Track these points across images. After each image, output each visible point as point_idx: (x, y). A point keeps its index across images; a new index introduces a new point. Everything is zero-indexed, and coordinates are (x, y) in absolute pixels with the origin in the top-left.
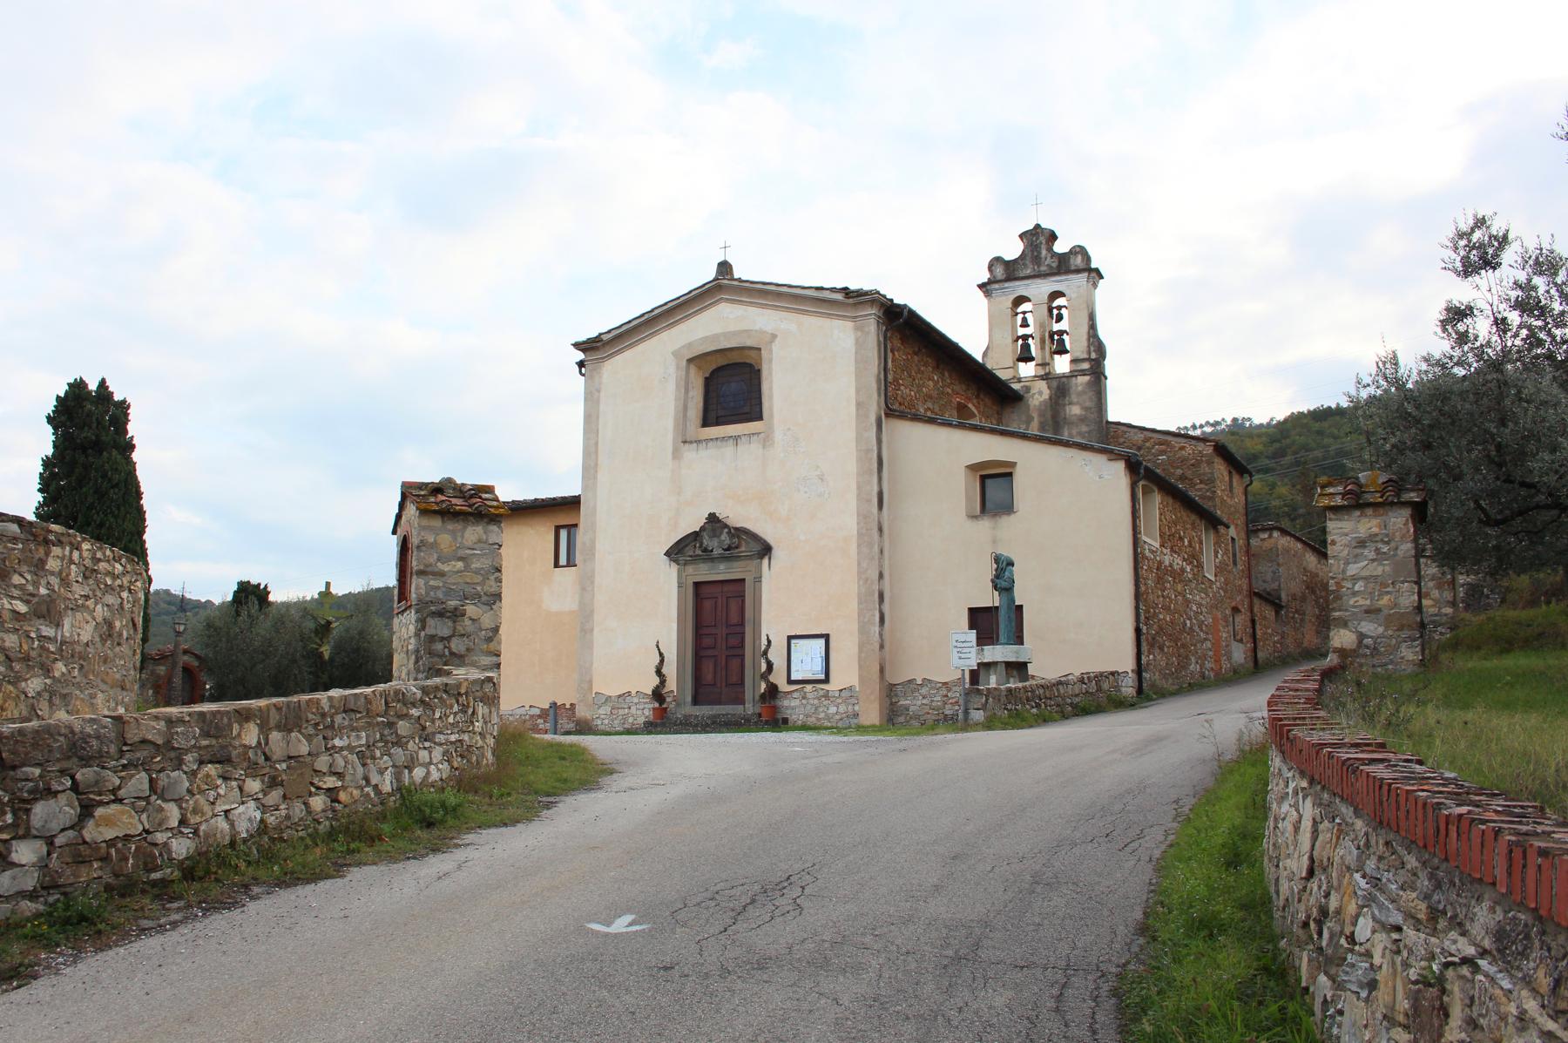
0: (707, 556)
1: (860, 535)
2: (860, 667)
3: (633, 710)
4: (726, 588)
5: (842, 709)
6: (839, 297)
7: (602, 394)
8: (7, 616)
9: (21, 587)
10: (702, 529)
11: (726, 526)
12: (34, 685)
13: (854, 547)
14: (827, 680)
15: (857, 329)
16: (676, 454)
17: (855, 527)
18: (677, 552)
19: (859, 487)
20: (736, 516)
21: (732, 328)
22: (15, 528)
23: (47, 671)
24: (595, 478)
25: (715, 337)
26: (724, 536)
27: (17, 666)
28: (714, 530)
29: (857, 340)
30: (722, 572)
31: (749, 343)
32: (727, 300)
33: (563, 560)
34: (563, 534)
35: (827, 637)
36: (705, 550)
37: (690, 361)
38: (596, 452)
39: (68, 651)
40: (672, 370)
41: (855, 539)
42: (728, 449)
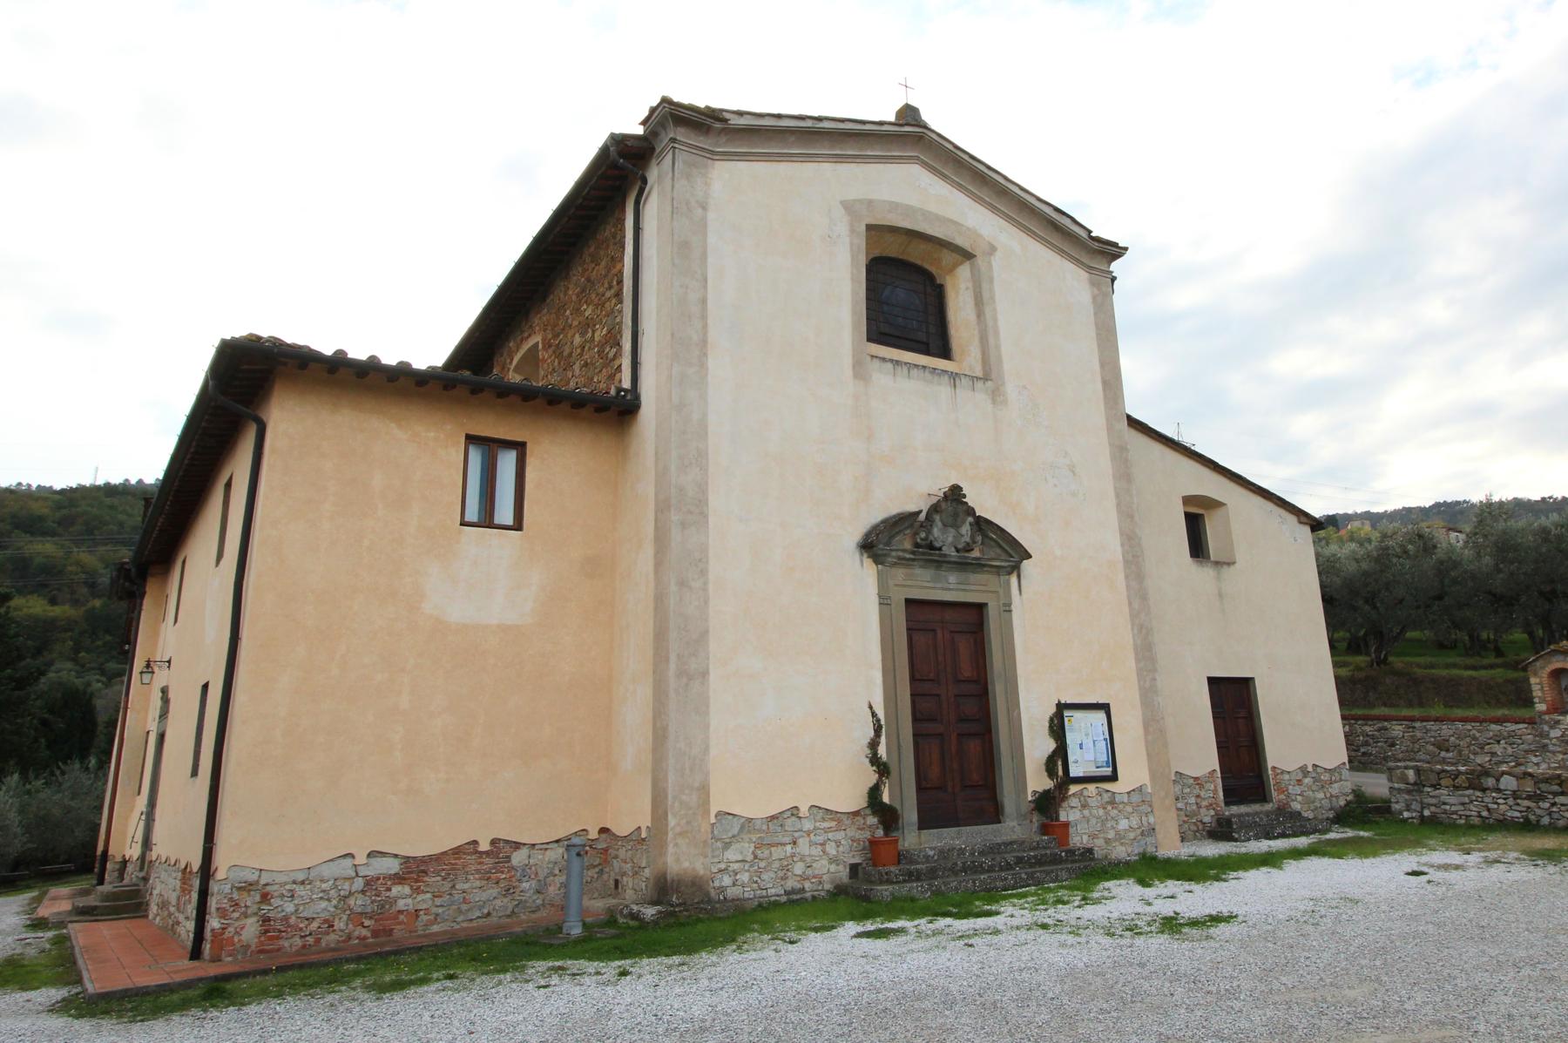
0: (928, 554)
1: (1126, 562)
2: (1148, 755)
3: (804, 847)
4: (949, 615)
5: (1135, 822)
6: (1083, 234)
7: (711, 215)
10: (935, 509)
11: (971, 511)
13: (1121, 577)
14: (1113, 777)
15: (1092, 283)
16: (859, 372)
17: (1119, 549)
18: (873, 545)
19: (1117, 496)
20: (983, 501)
21: (932, 208)
24: (702, 365)
25: (909, 210)
26: (966, 529)
28: (955, 515)
29: (1094, 298)
30: (950, 588)
31: (959, 241)
32: (925, 165)
33: (504, 513)
34: (475, 457)
35: (1105, 708)
36: (931, 547)
37: (869, 227)
38: (704, 317)
40: (842, 228)
41: (1120, 566)
42: (943, 390)
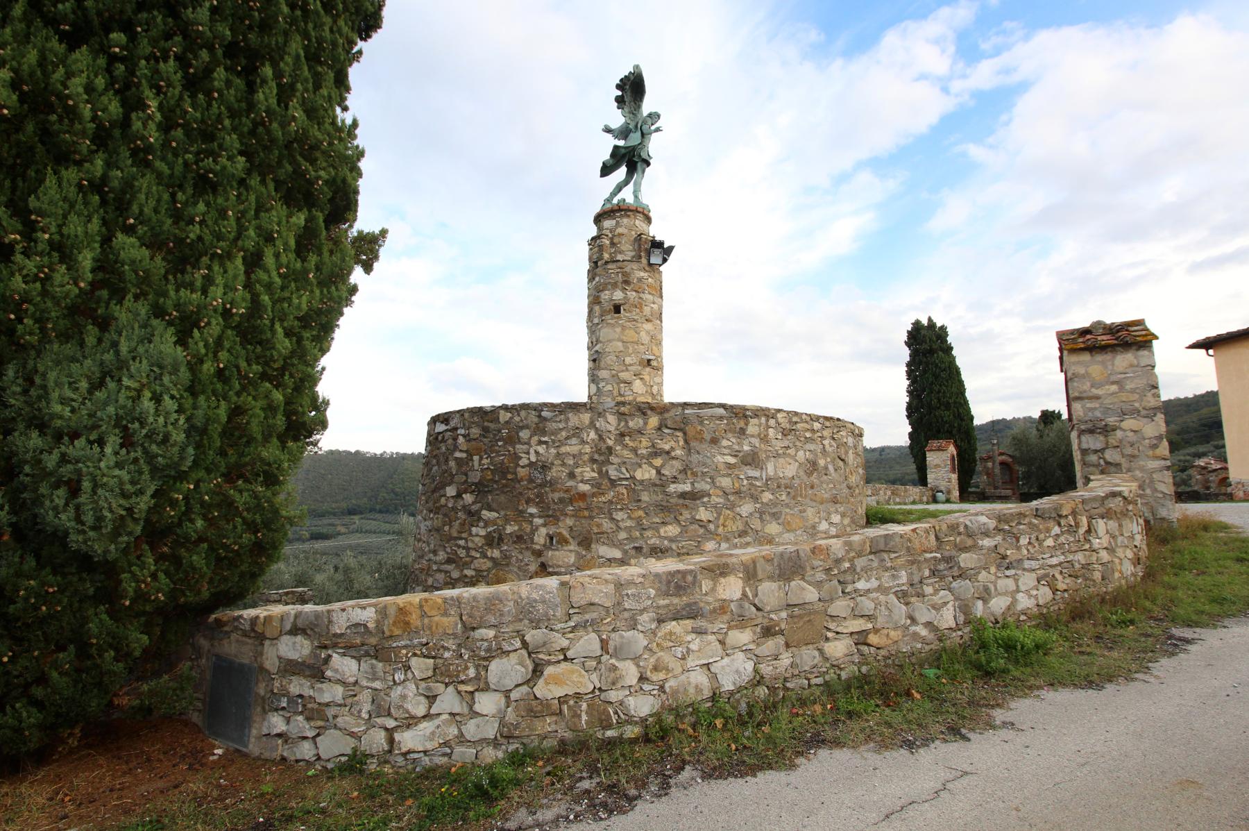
8: (722, 467)
9: (728, 447)
12: (746, 508)
22: (722, 411)
23: (755, 499)
27: (732, 498)
39: (775, 484)
